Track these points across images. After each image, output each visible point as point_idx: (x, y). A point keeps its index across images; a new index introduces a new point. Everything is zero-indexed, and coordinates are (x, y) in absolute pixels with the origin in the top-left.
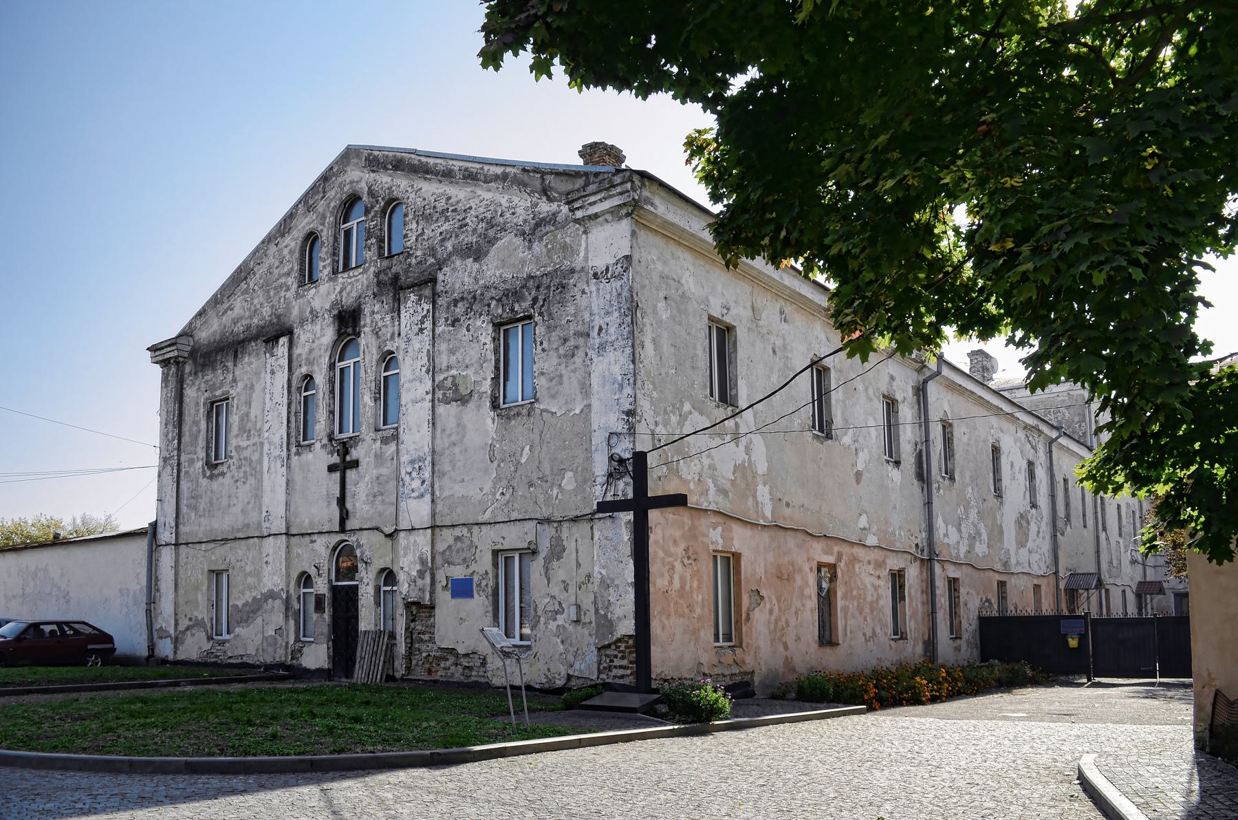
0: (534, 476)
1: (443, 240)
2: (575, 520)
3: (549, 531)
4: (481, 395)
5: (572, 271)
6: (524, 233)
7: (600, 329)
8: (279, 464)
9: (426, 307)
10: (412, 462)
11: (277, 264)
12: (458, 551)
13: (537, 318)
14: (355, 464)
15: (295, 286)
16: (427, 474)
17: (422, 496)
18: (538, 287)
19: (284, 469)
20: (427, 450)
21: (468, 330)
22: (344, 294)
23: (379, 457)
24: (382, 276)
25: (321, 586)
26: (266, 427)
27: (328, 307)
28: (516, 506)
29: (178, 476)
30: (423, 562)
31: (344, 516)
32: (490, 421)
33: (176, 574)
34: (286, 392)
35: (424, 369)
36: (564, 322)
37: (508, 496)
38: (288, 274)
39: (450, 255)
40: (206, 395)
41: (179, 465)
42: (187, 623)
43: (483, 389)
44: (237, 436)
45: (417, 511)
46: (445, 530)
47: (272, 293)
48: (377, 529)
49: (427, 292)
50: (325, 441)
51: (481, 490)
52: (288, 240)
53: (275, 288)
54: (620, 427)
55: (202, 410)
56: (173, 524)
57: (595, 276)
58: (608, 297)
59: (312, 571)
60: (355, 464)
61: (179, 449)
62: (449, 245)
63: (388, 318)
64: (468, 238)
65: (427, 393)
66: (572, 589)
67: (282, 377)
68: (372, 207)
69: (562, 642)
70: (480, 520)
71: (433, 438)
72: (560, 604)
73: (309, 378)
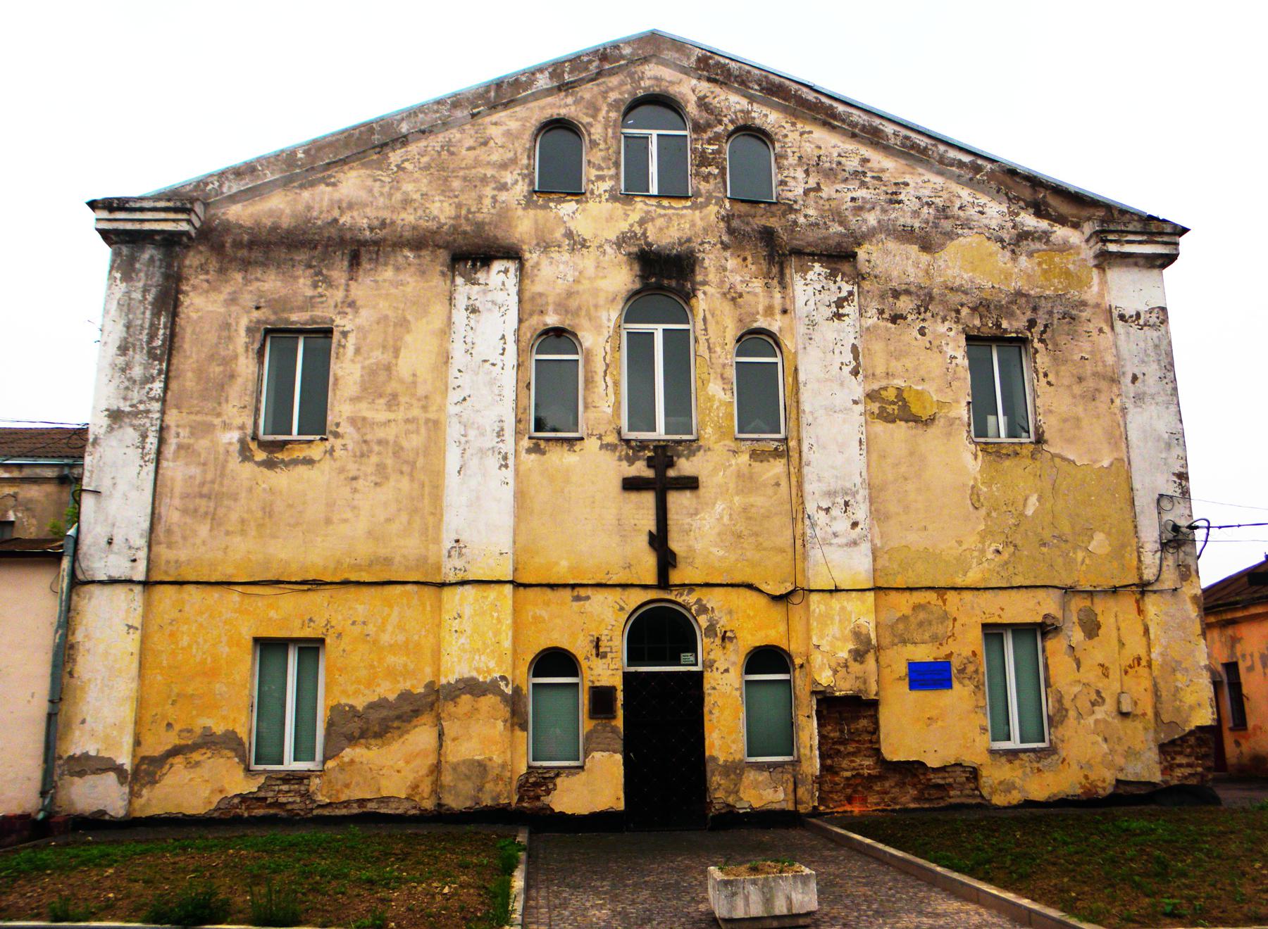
0: (1047, 534)
1: (861, 208)
2: (1115, 591)
3: (1077, 603)
4: (951, 422)
5: (1084, 304)
6: (1002, 241)
7: (1135, 378)
8: (493, 462)
9: (846, 288)
10: (831, 494)
11: (471, 142)
12: (921, 624)
13: (1037, 344)
14: (691, 484)
15: (521, 188)
16: (861, 512)
17: (855, 543)
18: (1035, 309)
19: (509, 474)
20: (858, 480)
21: (922, 332)
22: (650, 226)
23: (746, 482)
24: (735, 223)
25: (608, 671)
27: (614, 238)
28: (1020, 568)
29: (159, 452)
30: (857, 635)
32: (970, 457)
34: (512, 348)
35: (847, 370)
36: (1077, 357)
37: (1006, 556)
38: (504, 166)
40: (256, 314)
41: (162, 430)
42: (172, 740)
43: (952, 414)
44: (354, 400)
45: (854, 565)
46: (893, 594)
47: (456, 184)
48: (750, 587)
49: (846, 267)
50: (611, 438)
51: (960, 543)
53: (465, 179)
54: (1171, 489)
56: (142, 542)
57: (1122, 317)
58: (1142, 345)
59: (579, 647)
60: (691, 484)
61: (163, 400)
62: (872, 219)
64: (903, 217)
65: (855, 402)
66: (1115, 673)
68: (709, 125)
69: (1106, 740)
70: (960, 582)
72: (1098, 692)
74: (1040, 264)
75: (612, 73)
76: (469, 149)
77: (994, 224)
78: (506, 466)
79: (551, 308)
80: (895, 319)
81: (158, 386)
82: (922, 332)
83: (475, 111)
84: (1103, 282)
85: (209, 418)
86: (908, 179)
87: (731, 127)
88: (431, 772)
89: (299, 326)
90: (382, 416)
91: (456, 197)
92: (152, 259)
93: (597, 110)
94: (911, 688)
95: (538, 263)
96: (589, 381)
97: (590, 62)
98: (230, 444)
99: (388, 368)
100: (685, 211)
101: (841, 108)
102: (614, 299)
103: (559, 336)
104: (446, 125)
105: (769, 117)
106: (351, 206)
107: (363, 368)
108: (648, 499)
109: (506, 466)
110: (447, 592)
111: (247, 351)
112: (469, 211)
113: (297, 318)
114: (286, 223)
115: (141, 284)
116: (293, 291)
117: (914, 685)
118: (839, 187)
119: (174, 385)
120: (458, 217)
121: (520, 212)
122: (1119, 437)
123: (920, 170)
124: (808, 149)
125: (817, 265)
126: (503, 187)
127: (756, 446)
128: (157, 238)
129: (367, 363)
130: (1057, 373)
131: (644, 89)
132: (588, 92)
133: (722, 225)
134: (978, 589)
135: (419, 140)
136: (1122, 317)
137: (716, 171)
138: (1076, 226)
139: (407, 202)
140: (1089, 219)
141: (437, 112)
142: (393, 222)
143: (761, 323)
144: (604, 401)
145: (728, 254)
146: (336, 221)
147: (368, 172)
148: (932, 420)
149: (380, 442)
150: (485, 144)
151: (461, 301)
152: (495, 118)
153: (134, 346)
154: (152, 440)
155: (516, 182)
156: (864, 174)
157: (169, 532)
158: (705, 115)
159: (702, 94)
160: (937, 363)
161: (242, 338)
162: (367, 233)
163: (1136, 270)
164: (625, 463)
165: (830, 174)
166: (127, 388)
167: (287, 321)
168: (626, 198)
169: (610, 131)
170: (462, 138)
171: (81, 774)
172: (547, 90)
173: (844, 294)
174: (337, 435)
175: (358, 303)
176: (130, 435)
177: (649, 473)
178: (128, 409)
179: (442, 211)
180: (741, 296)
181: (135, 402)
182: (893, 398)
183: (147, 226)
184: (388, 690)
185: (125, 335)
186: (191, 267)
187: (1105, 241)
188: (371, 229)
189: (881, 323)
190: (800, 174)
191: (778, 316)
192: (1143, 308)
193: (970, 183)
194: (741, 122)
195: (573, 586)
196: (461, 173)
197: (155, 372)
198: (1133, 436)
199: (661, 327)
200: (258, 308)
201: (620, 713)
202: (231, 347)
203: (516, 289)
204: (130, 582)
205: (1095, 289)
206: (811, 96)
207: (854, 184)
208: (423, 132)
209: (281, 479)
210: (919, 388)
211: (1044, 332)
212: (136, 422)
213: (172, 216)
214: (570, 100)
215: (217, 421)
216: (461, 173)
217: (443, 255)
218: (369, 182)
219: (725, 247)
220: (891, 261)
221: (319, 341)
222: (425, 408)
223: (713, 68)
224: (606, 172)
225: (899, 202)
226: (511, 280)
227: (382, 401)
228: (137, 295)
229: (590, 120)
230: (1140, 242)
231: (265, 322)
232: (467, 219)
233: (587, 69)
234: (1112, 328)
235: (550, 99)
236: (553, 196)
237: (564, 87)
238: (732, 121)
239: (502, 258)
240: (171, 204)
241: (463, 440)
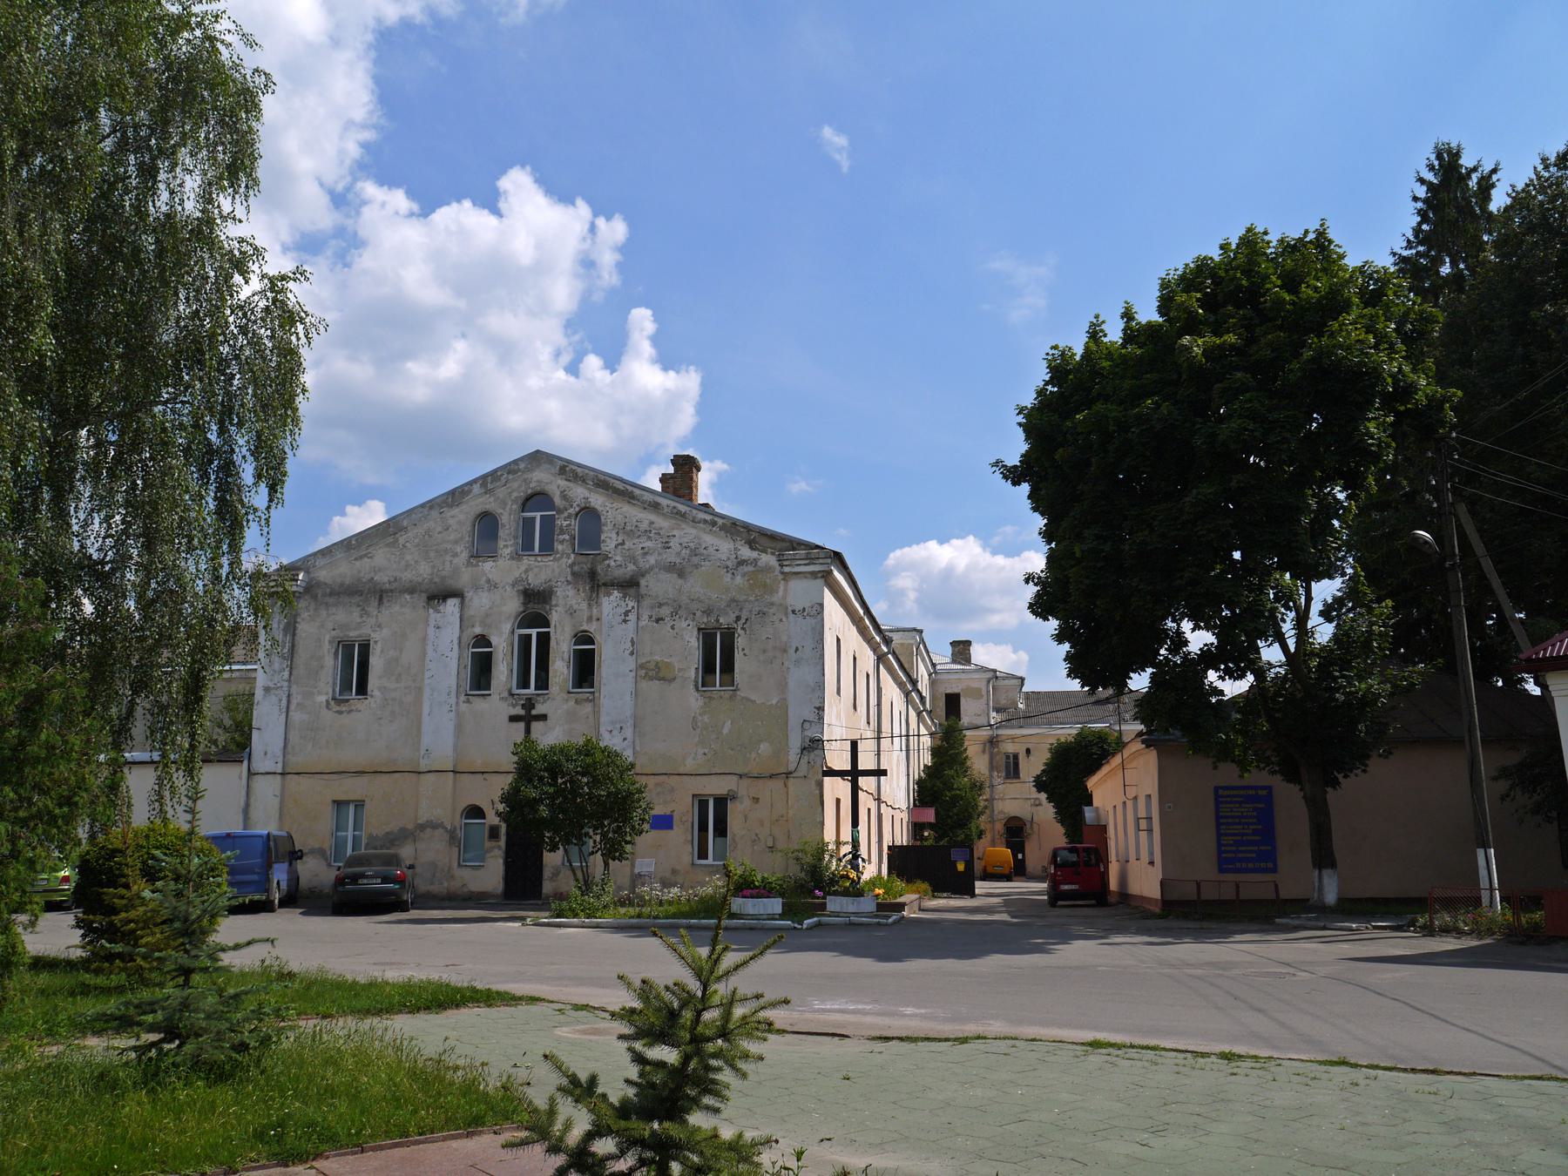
9: (631, 604)
10: (613, 723)
14: (543, 717)
15: (465, 555)
16: (628, 733)
19: (452, 715)
24: (576, 568)
26: (427, 674)
33: (282, 802)
34: (456, 647)
38: (456, 542)
39: (651, 568)
44: (380, 678)
47: (432, 554)
49: (632, 591)
50: (506, 694)
52: (449, 513)
54: (812, 717)
55: (327, 650)
56: (280, 754)
60: (543, 717)
62: (652, 560)
63: (584, 605)
67: (451, 633)
71: (636, 705)
73: (482, 640)
80: (657, 621)
81: (286, 674)
84: (786, 590)
101: (637, 492)
103: (482, 640)
105: (598, 500)
108: (522, 725)
116: (347, 620)
122: (783, 686)
132: (501, 492)
139: (407, 566)
143: (585, 627)
144: (504, 672)
149: (394, 700)
151: (432, 623)
154: (284, 702)
161: (326, 646)
165: (630, 534)
168: (516, 557)
176: (274, 699)
177: (522, 712)
184: (394, 826)
190: (614, 536)
192: (807, 605)
198: (792, 684)
201: (503, 838)
206: (620, 486)
207: (643, 539)
209: (345, 720)
217: (424, 596)
220: (658, 585)
223: (568, 470)
226: (457, 610)
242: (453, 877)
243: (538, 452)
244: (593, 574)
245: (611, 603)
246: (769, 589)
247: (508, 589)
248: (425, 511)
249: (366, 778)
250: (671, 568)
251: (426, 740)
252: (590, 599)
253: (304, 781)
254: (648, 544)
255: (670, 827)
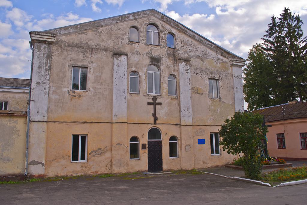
4: (206, 94)
5: (228, 73)
6: (215, 60)
7: (236, 88)
9: (188, 67)
10: (185, 107)
11: (116, 29)
14: (160, 104)
16: (190, 111)
17: (189, 117)
18: (220, 74)
21: (201, 77)
22: (152, 51)
23: (170, 104)
24: (168, 52)
26: (114, 84)
27: (145, 53)
29: (49, 92)
31: (156, 119)
32: (208, 101)
34: (126, 75)
36: (227, 83)
38: (123, 35)
39: (193, 56)
44: (93, 83)
47: (113, 37)
49: (188, 63)
57: (235, 76)
59: (139, 136)
60: (160, 104)
62: (193, 54)
63: (172, 65)
64: (198, 54)
65: (190, 90)
68: (164, 31)
74: (221, 65)
75: (145, 17)
76: (116, 30)
77: (214, 57)
78: (125, 99)
79: (133, 67)
81: (48, 77)
82: (201, 77)
83: (117, 22)
84: (232, 70)
85: (60, 85)
86: (199, 46)
87: (168, 32)
88: (110, 161)
89: (80, 66)
90: (99, 87)
91: (113, 40)
92: (45, 47)
93: (142, 25)
94: (198, 144)
95: (131, 57)
96: (141, 82)
97: (141, 14)
98: (65, 91)
99: (100, 77)
100: (159, 49)
102: (146, 66)
104: (111, 24)
105: (174, 31)
106: (90, 40)
107: (95, 76)
109: (125, 99)
110: (114, 124)
111: (68, 70)
112: (116, 44)
113: (80, 64)
114: (76, 42)
115: (43, 53)
117: (199, 143)
118: (187, 47)
119: (51, 77)
120: (114, 45)
121: (127, 45)
123: (201, 45)
124: (182, 38)
125: (183, 62)
126: (123, 39)
127: (172, 97)
128: (46, 42)
129: (96, 75)
130: (224, 86)
131: (151, 22)
132: (140, 21)
133: (166, 52)
134: (209, 126)
135: (104, 27)
136: (235, 76)
137: (165, 41)
138: (227, 58)
139: (103, 40)
140: (230, 57)
141: (109, 21)
142: (100, 45)
143: (173, 73)
144: (144, 86)
145: (167, 58)
146: (87, 43)
147: (94, 32)
148: (203, 94)
149: (99, 93)
150: (119, 29)
151: (115, 64)
152: (121, 24)
153: (42, 67)
154: (47, 90)
155: (126, 39)
156: (191, 44)
157: (52, 110)
158: (163, 29)
159: (162, 24)
160: (204, 83)
162: (95, 46)
163: (237, 68)
164: (148, 99)
165: (186, 44)
166: (41, 77)
167: (77, 64)
169: (144, 30)
170: (115, 27)
171: (33, 164)
172: (132, 19)
173: (188, 68)
174: (89, 90)
175: (93, 62)
177: (152, 102)
178: (41, 82)
179: (110, 43)
180: (169, 67)
181: (43, 80)
182: (196, 89)
183: (44, 39)
185: (39, 64)
186: (54, 50)
187: (233, 62)
188: (95, 46)
189: (194, 74)
190: (180, 44)
191: (176, 72)
192: (238, 75)
193: (210, 48)
194: (169, 31)
195: (138, 124)
196: (114, 35)
197: (47, 74)
199: (154, 72)
200: (71, 61)
202: (65, 69)
203: (127, 62)
204: (43, 121)
205: (230, 70)
206: (183, 27)
207: (189, 46)
208: (106, 25)
210: (200, 87)
211: (222, 78)
212: (43, 85)
213: (51, 38)
214: (136, 22)
215: (62, 86)
216: (114, 35)
217: (111, 53)
218: (94, 35)
219: (166, 57)
221: (84, 70)
222: (108, 86)
224: (144, 39)
225: (198, 51)
227: (99, 84)
228: (42, 55)
229: (140, 27)
230: (239, 63)
231: (73, 64)
232: (116, 46)
233: (140, 16)
234: (233, 78)
235: (132, 21)
236: (133, 43)
237: (135, 19)
238: (168, 31)
239: (123, 55)
240: (50, 35)
241: (117, 93)
242: (128, 165)
243: (153, 9)
244: (174, 55)
245: (182, 65)
246: (227, 69)
247: (145, 56)
248: (111, 20)
249: (87, 125)
250: (199, 57)
251: (115, 110)
252: (174, 64)
253: (56, 124)
254: (191, 48)
255: (204, 143)
